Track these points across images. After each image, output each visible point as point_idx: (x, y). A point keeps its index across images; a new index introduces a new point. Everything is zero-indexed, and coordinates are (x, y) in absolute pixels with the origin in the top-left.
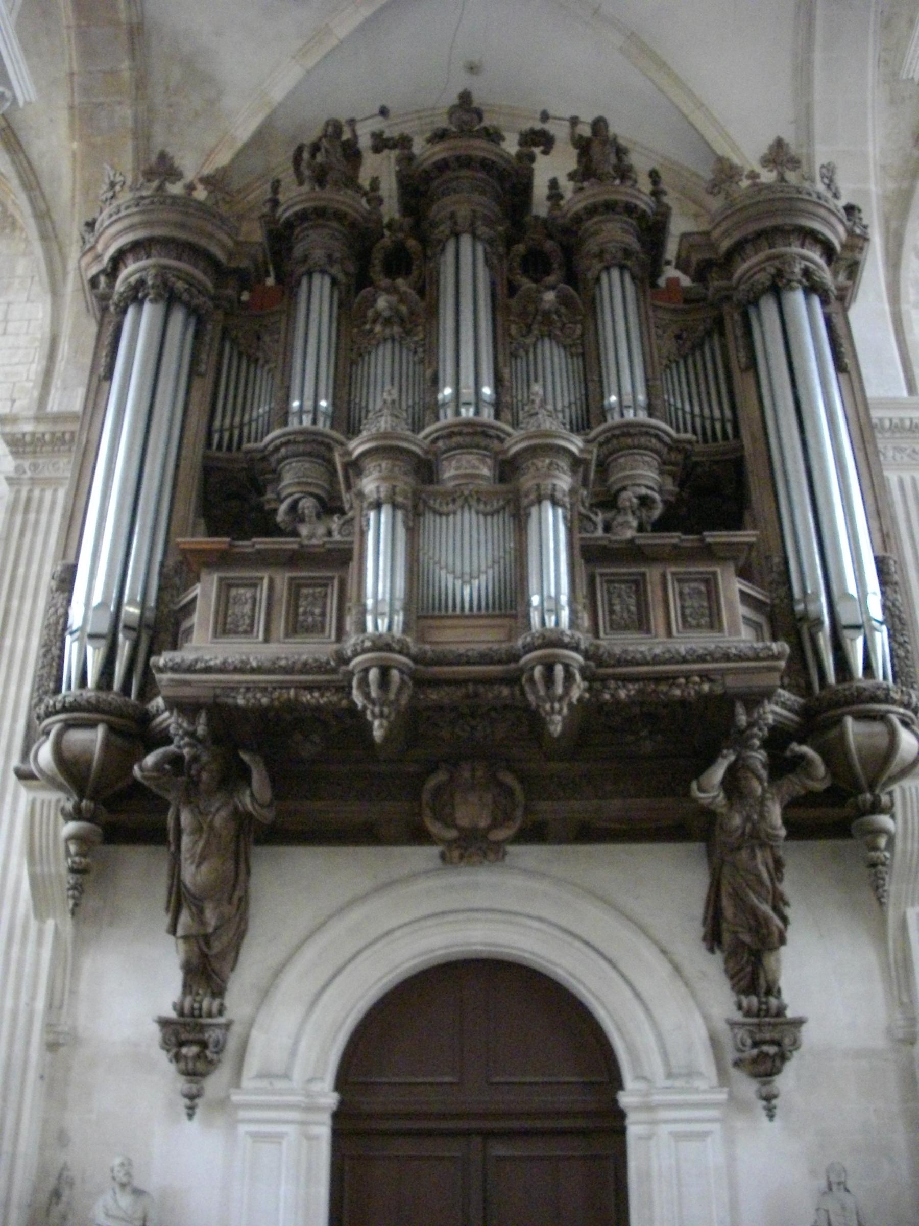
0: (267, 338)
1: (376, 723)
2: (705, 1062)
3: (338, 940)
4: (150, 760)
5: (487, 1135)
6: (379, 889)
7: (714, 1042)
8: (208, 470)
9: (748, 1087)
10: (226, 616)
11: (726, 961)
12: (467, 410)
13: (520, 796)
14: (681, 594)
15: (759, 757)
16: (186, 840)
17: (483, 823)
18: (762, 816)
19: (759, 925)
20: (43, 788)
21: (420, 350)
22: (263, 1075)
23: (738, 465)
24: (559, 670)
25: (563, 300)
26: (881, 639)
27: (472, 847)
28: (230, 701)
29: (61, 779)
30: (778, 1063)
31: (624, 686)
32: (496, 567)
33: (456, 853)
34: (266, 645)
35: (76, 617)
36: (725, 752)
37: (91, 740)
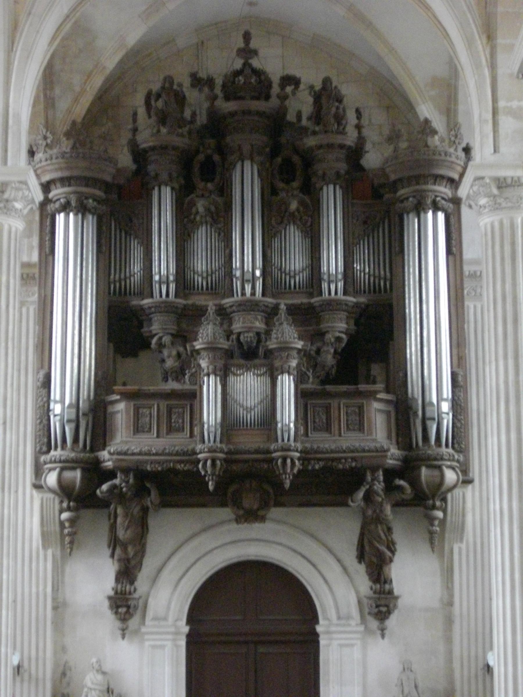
0: (135, 221)
1: (210, 483)
2: (355, 612)
3: (188, 556)
4: (105, 487)
5: (256, 643)
6: (204, 530)
7: (360, 602)
8: (110, 308)
9: (374, 624)
10: (138, 423)
11: (367, 567)
12: (248, 286)
13: (272, 496)
14: (347, 413)
15: (379, 487)
16: (119, 520)
17: (255, 507)
18: (381, 511)
20: (45, 492)
21: (222, 234)
22: (156, 618)
23: (391, 306)
24: (289, 461)
25: (302, 203)
26: (447, 421)
28: (144, 468)
29: (61, 494)
30: (387, 614)
31: (318, 463)
32: (262, 404)
33: (243, 520)
34: (157, 440)
35: (57, 408)
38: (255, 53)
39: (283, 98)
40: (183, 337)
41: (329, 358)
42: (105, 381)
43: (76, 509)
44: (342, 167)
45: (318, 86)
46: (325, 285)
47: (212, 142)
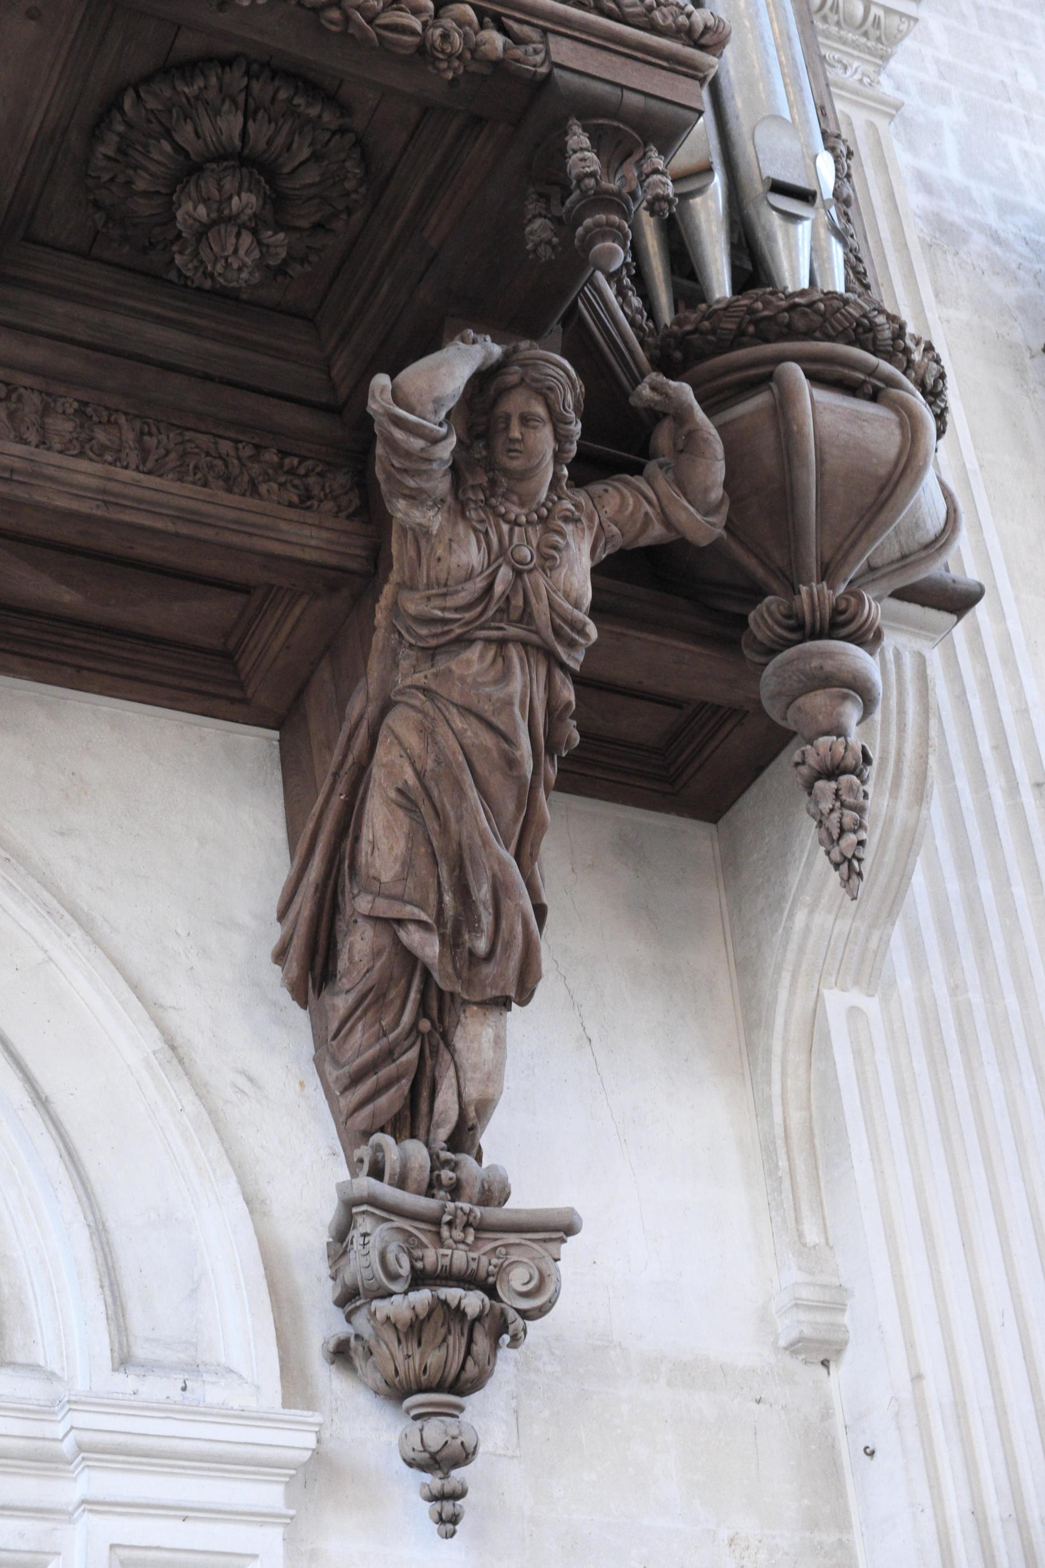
2: (241, 1334)
9: (372, 1432)
30: (482, 1344)
36: (471, 333)
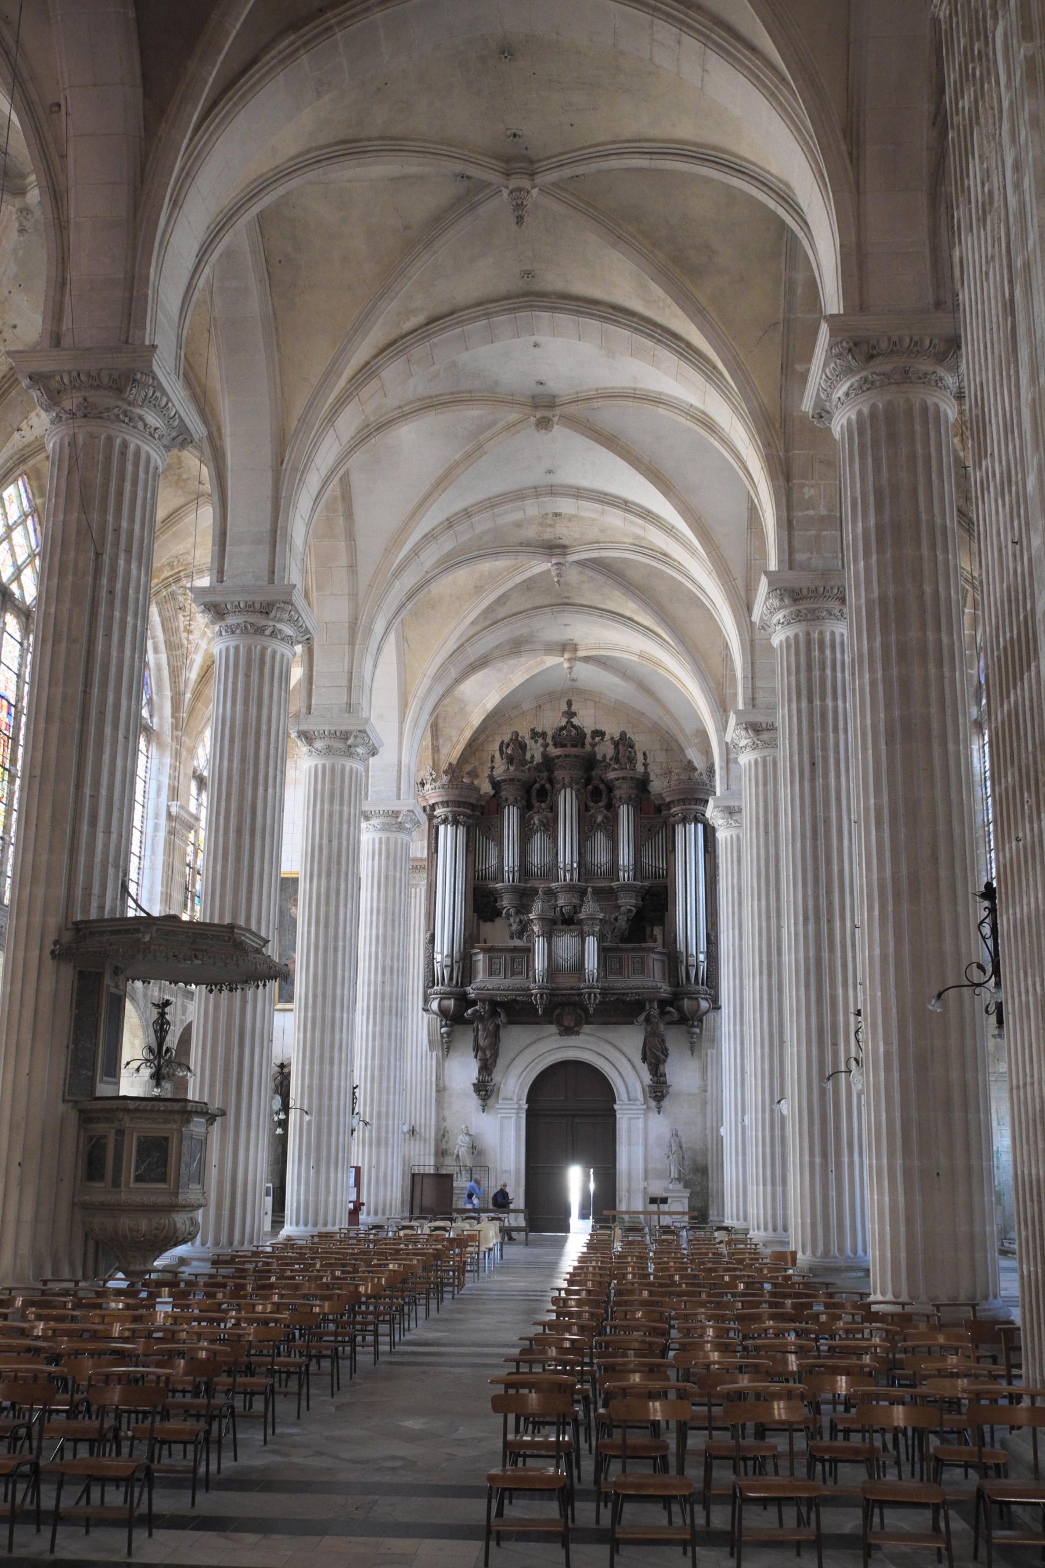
2: (640, 1096)
5: (573, 1116)
9: (653, 1103)
15: (655, 1011)
19: (657, 1057)
25: (606, 817)
26: (703, 967)
27: (568, 1031)
35: (438, 957)
37: (451, 1003)
38: (575, 714)
39: (594, 745)
40: (523, 908)
41: (622, 923)
42: (471, 939)
43: (451, 1026)
44: (634, 793)
45: (617, 736)
46: (621, 874)
47: (545, 774)
